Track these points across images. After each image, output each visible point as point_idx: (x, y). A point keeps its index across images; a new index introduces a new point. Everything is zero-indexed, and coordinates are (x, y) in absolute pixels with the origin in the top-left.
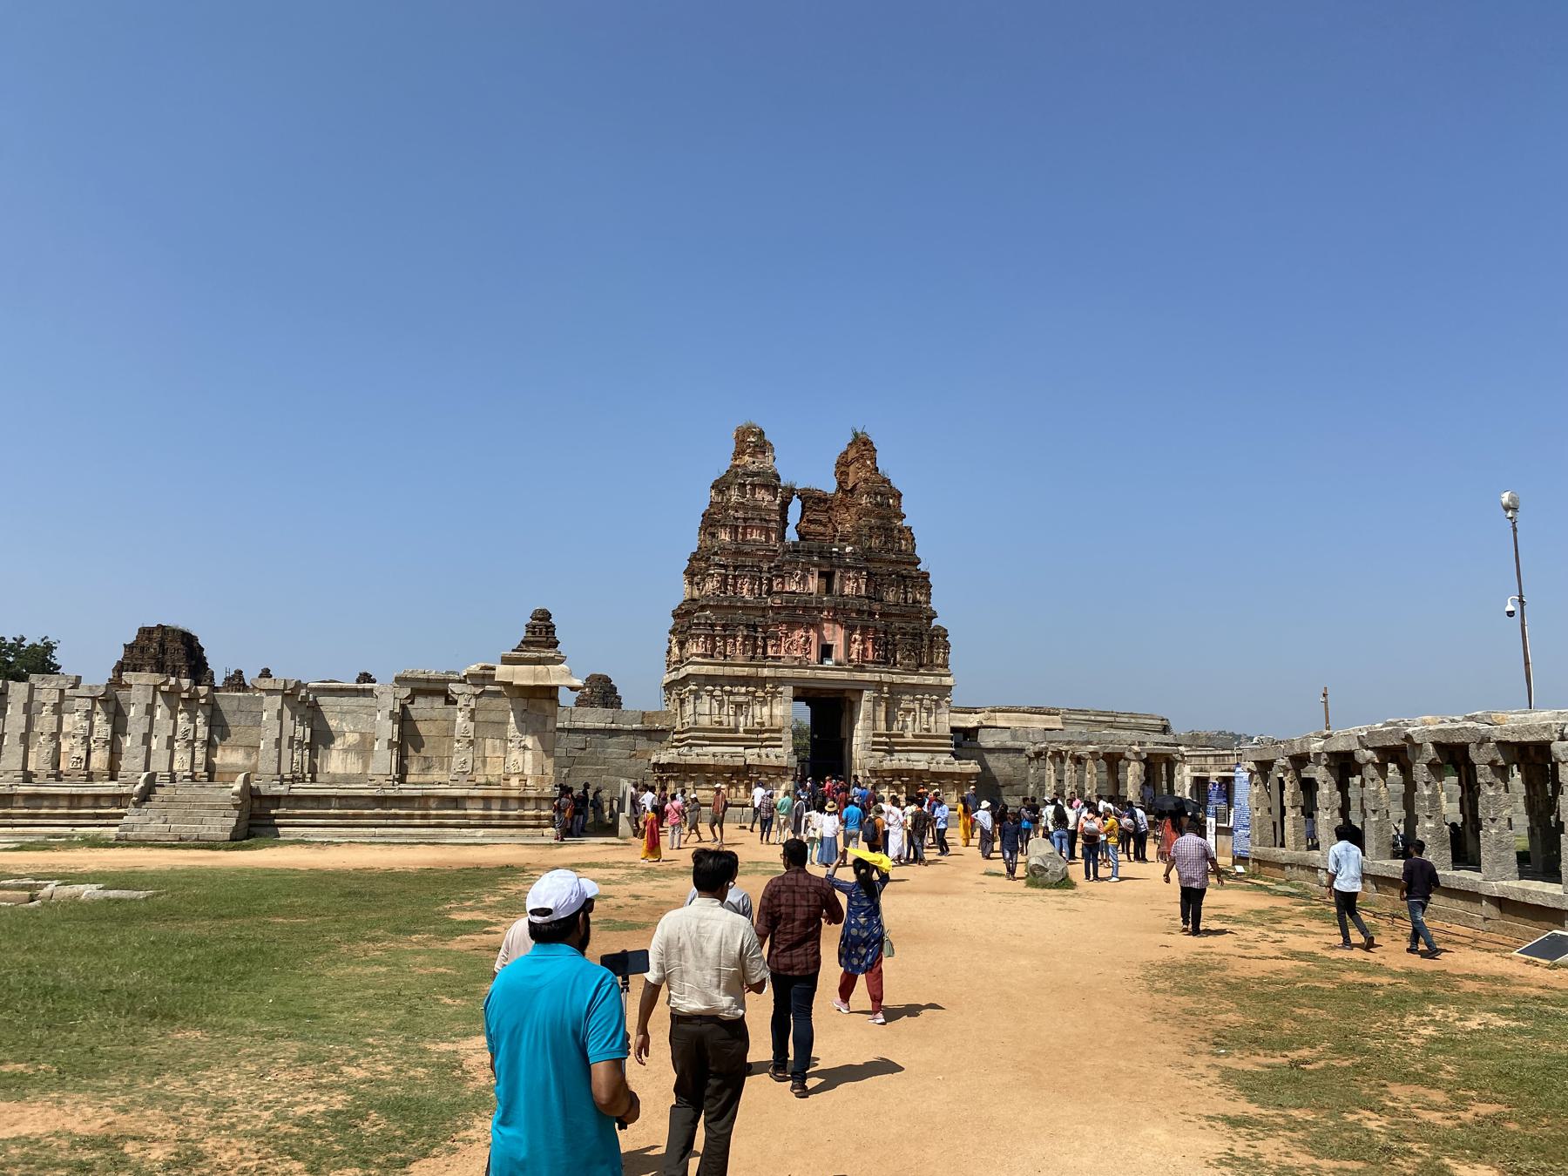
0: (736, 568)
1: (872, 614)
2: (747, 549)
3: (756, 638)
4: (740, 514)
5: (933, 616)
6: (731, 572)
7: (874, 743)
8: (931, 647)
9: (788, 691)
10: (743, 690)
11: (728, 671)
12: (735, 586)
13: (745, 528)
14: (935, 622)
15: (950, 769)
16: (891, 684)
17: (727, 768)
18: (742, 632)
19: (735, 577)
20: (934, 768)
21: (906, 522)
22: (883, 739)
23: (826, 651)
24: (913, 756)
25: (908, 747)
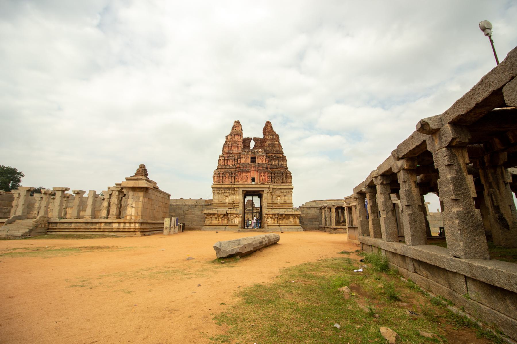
0: (227, 157)
1: (267, 168)
3: (232, 177)
4: (230, 143)
6: (226, 158)
9: (241, 191)
10: (228, 191)
11: (223, 186)
15: (291, 213)
17: (221, 214)
18: (227, 175)
20: (286, 213)
22: (271, 205)
23: (253, 180)
24: (281, 210)
25: (279, 207)
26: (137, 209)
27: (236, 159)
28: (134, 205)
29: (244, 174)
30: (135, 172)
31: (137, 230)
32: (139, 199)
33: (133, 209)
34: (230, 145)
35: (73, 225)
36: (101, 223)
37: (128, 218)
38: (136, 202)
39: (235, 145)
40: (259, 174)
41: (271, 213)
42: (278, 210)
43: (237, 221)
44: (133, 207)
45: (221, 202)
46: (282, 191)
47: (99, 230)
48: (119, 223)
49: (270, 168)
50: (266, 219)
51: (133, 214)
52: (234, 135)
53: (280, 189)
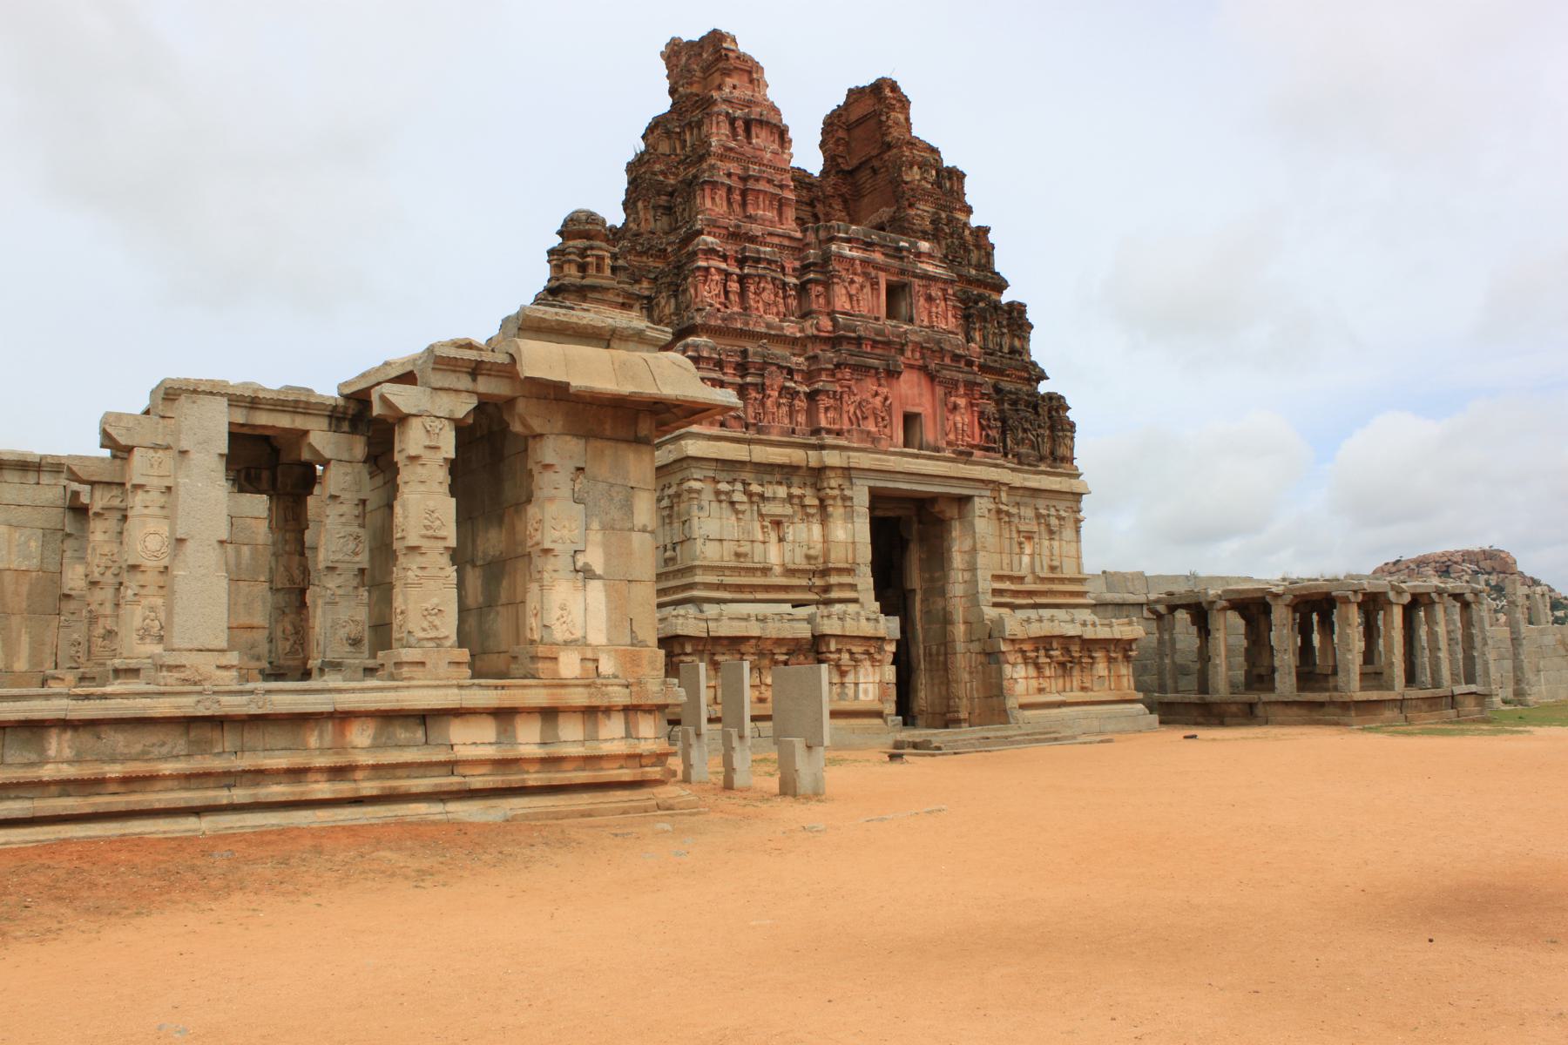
0: (741, 262)
2: (756, 229)
5: (1042, 376)
7: (996, 592)
8: (1052, 428)
10: (782, 491)
11: (762, 454)
12: (743, 293)
13: (744, 193)
14: (1043, 388)
15: (1103, 633)
16: (1012, 488)
17: (779, 642)
19: (742, 280)
20: (1089, 634)
21: (975, 221)
22: (1006, 585)
26: (619, 584)
27: (792, 280)
28: (594, 558)
29: (870, 385)
30: (540, 275)
31: (654, 772)
32: (628, 507)
33: (596, 590)
34: (734, 183)
35: (57, 744)
36: (343, 718)
37: (569, 665)
38: (604, 528)
39: (762, 186)
40: (940, 391)
41: (1036, 630)
42: (1033, 614)
43: (872, 683)
44: (587, 573)
45: (741, 564)
46: (1041, 504)
47: (343, 788)
48: (504, 715)
49: (981, 367)
50: (1007, 669)
51: (598, 637)
52: (748, 124)
53: (1035, 492)
